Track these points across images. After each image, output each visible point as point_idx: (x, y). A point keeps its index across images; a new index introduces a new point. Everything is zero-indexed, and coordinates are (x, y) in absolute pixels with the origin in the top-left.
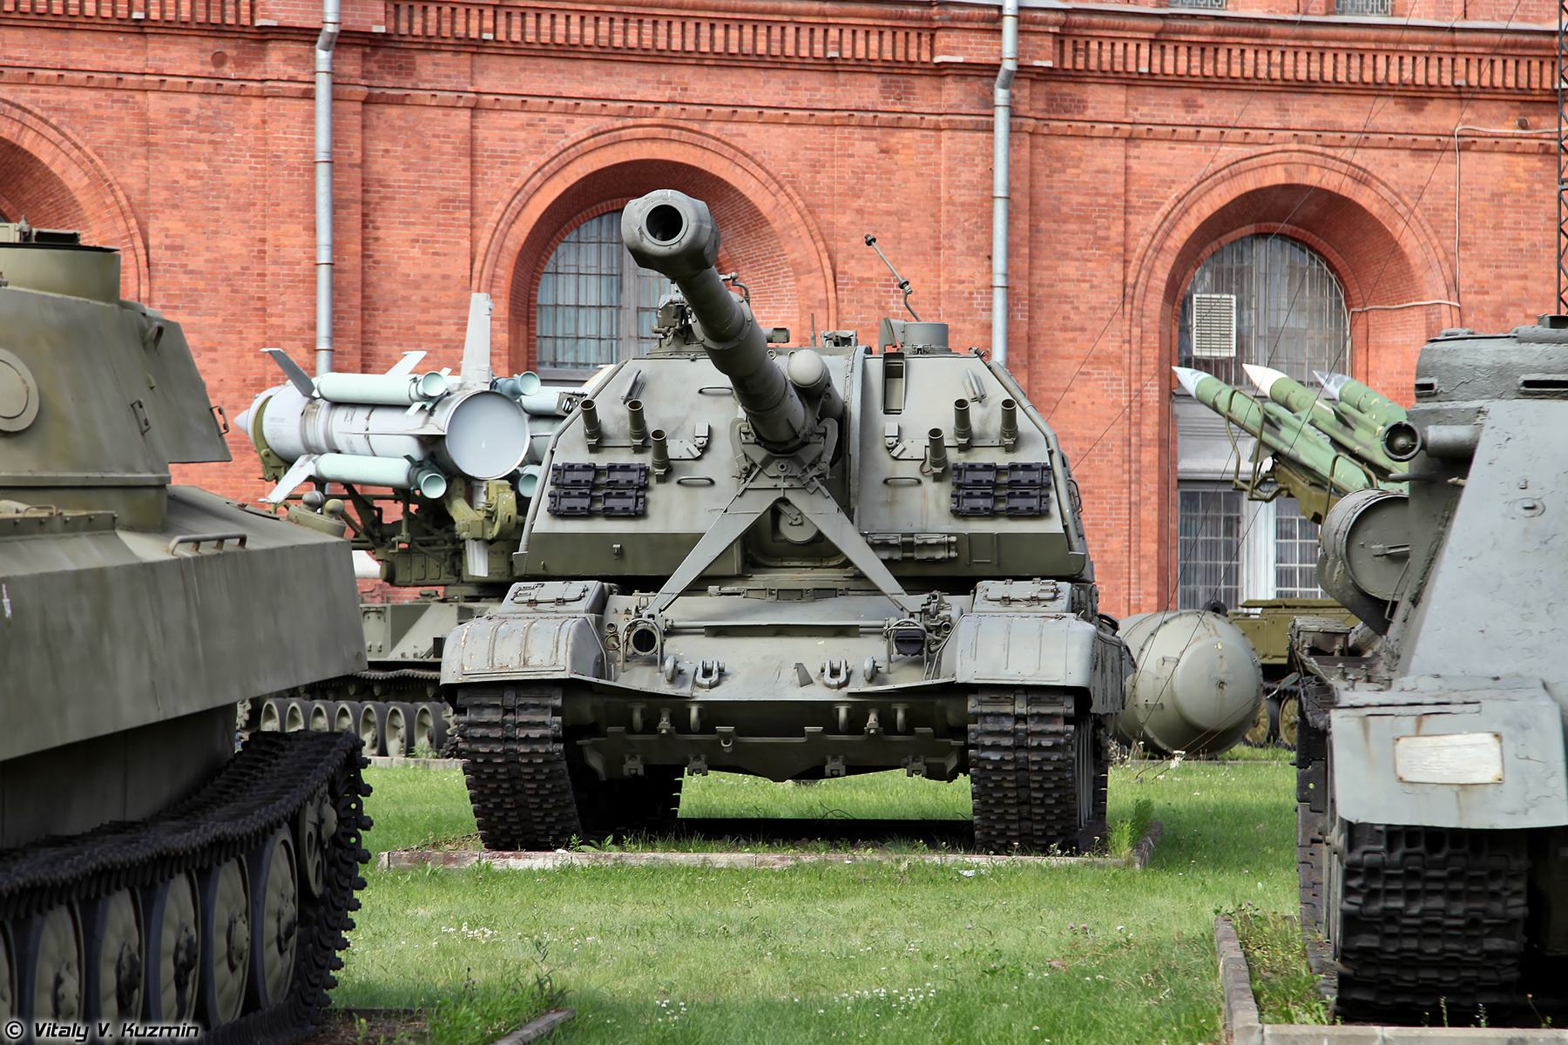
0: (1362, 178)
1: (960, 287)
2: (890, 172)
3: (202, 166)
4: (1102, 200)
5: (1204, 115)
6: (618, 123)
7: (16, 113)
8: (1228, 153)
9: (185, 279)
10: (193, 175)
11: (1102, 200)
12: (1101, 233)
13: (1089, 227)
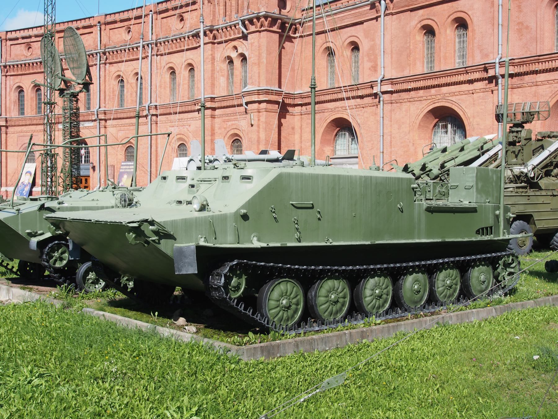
3: (483, 107)
10: (482, 109)
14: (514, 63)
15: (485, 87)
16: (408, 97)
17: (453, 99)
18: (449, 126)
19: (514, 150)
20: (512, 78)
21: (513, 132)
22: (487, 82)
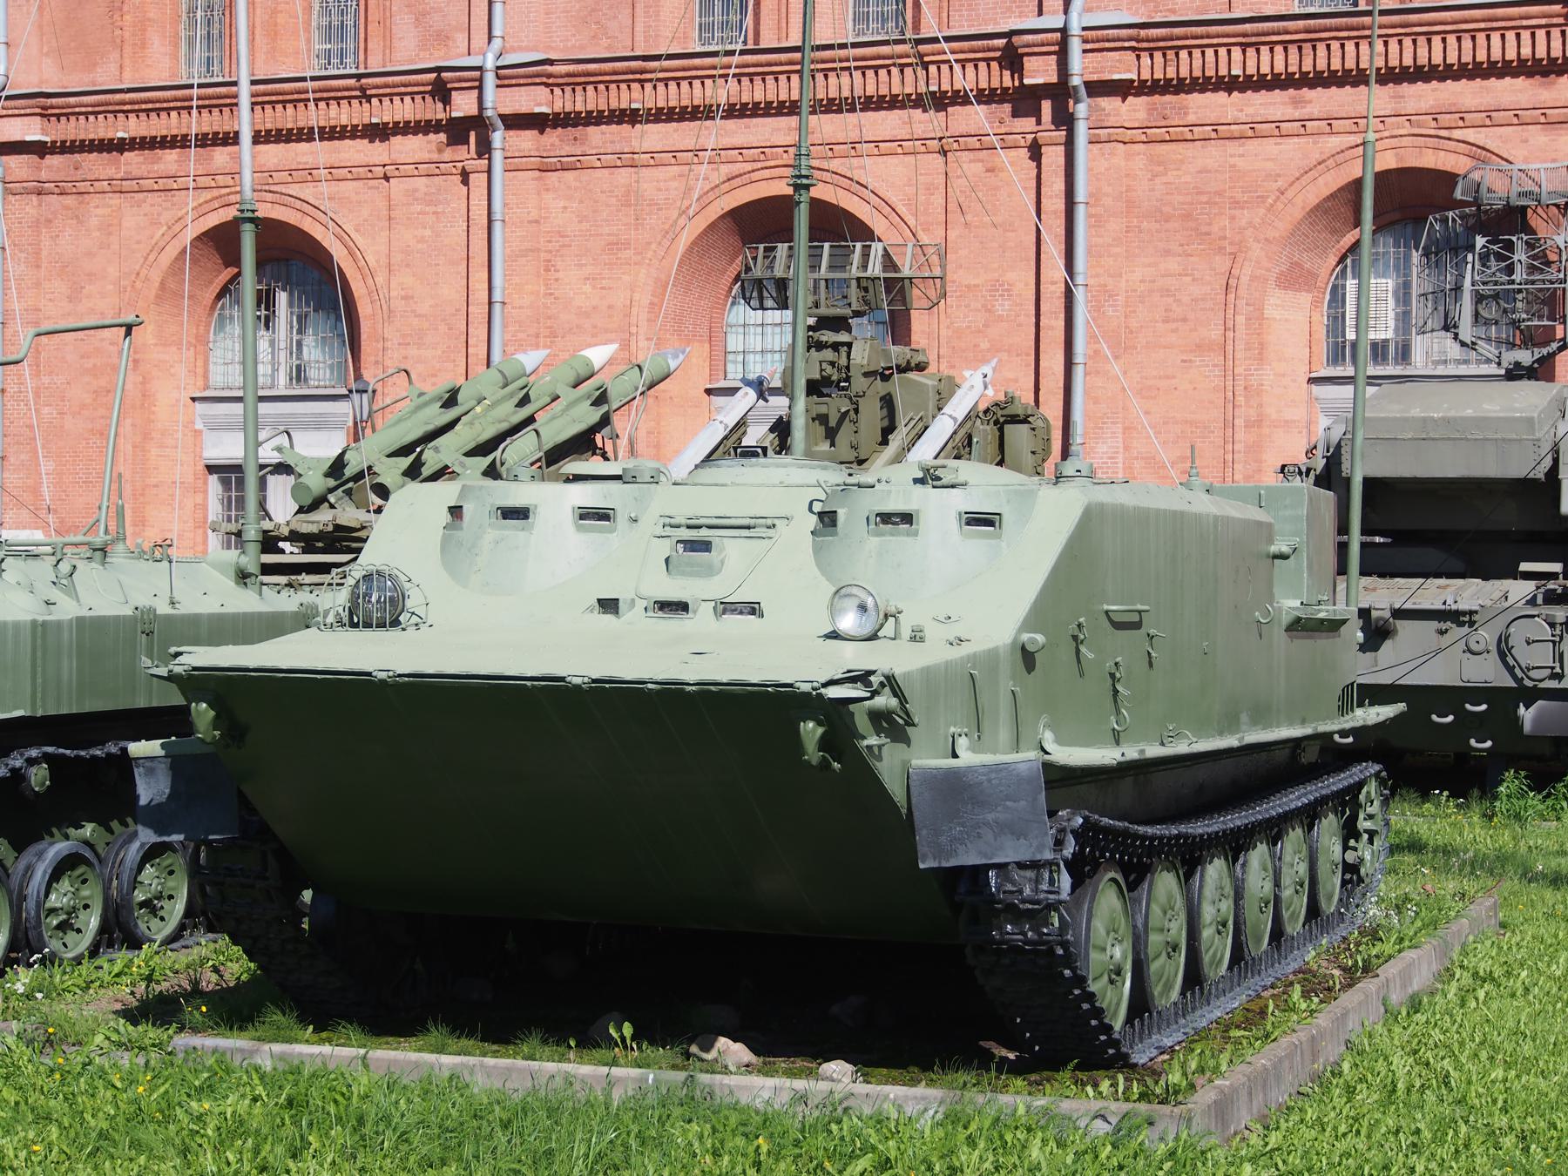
0: (1481, 154)
1: (1053, 288)
2: (997, 188)
3: (428, 232)
4: (1204, 198)
5: (1313, 110)
6: (749, 167)
7: (298, 204)
8: (1335, 142)
9: (415, 322)
10: (421, 240)
11: (1204, 198)
12: (1204, 229)
13: (1192, 224)
14: (550, 76)
15: (435, 157)
16: (111, 172)
17: (307, 192)
18: (282, 298)
19: (823, 410)
20: (542, 132)
21: (820, 346)
22: (442, 137)
